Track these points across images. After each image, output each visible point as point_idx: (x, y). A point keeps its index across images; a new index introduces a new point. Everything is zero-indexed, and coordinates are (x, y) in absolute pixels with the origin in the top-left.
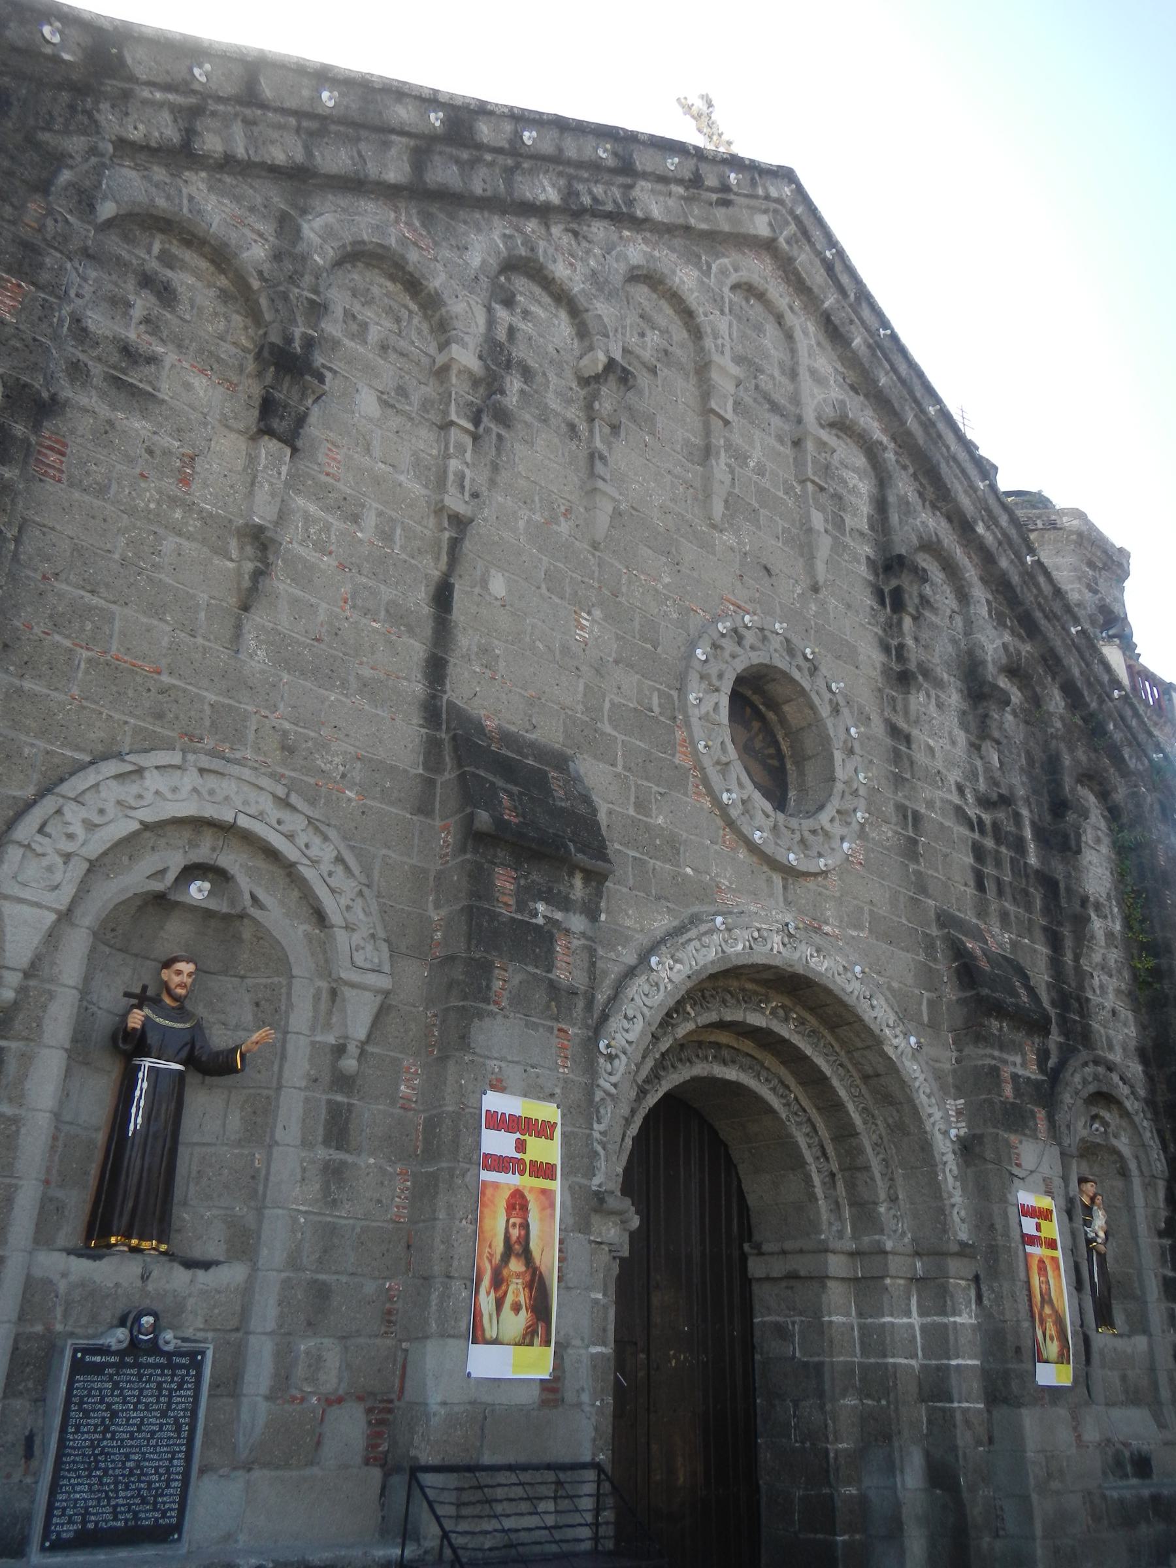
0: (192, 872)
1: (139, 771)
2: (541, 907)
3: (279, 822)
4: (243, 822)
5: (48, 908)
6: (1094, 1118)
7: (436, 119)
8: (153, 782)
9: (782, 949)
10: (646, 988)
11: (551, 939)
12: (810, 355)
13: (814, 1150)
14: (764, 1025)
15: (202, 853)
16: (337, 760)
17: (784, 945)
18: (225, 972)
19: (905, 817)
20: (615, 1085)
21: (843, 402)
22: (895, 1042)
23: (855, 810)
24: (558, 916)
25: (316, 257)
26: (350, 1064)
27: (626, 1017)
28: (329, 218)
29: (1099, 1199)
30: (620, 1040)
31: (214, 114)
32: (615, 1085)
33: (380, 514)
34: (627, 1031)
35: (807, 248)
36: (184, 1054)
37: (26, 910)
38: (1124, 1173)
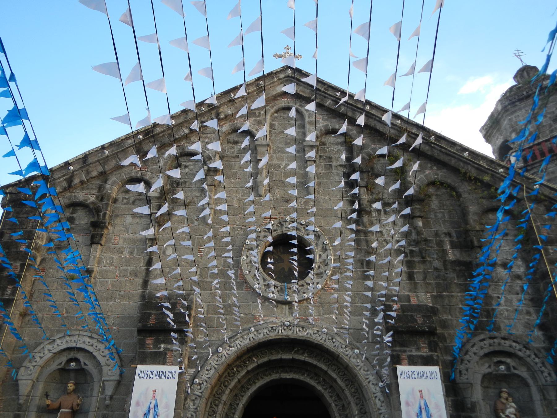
0: (69, 361)
1: (54, 341)
2: (162, 346)
3: (89, 343)
4: (78, 346)
5: (29, 380)
6: (501, 363)
7: (140, 137)
8: (58, 342)
9: (283, 331)
10: (216, 359)
11: (166, 354)
12: (309, 117)
13: (333, 398)
14: (291, 357)
15: (72, 355)
16: (111, 320)
17: (284, 330)
18: (85, 383)
19: (362, 264)
20: (201, 393)
21: (327, 125)
22: (347, 353)
23: (325, 271)
24: (169, 347)
25: (109, 191)
26: (107, 402)
27: (207, 370)
28: (114, 178)
29: (510, 399)
30: (205, 377)
31: (76, 174)
32: (201, 393)
33: (130, 248)
34: (208, 374)
35: (302, 84)
36: (70, 406)
37: (24, 381)
38: (527, 385)
